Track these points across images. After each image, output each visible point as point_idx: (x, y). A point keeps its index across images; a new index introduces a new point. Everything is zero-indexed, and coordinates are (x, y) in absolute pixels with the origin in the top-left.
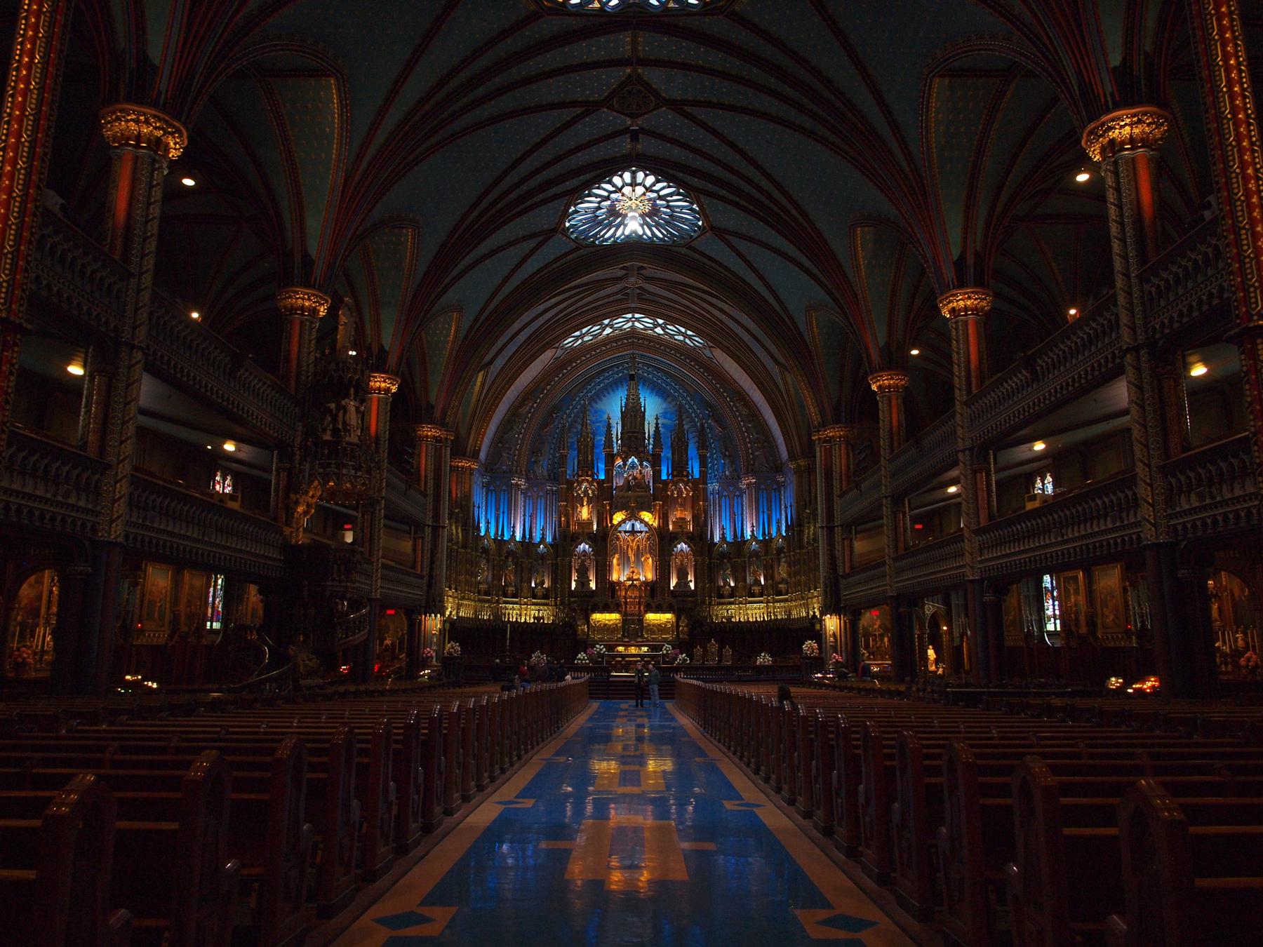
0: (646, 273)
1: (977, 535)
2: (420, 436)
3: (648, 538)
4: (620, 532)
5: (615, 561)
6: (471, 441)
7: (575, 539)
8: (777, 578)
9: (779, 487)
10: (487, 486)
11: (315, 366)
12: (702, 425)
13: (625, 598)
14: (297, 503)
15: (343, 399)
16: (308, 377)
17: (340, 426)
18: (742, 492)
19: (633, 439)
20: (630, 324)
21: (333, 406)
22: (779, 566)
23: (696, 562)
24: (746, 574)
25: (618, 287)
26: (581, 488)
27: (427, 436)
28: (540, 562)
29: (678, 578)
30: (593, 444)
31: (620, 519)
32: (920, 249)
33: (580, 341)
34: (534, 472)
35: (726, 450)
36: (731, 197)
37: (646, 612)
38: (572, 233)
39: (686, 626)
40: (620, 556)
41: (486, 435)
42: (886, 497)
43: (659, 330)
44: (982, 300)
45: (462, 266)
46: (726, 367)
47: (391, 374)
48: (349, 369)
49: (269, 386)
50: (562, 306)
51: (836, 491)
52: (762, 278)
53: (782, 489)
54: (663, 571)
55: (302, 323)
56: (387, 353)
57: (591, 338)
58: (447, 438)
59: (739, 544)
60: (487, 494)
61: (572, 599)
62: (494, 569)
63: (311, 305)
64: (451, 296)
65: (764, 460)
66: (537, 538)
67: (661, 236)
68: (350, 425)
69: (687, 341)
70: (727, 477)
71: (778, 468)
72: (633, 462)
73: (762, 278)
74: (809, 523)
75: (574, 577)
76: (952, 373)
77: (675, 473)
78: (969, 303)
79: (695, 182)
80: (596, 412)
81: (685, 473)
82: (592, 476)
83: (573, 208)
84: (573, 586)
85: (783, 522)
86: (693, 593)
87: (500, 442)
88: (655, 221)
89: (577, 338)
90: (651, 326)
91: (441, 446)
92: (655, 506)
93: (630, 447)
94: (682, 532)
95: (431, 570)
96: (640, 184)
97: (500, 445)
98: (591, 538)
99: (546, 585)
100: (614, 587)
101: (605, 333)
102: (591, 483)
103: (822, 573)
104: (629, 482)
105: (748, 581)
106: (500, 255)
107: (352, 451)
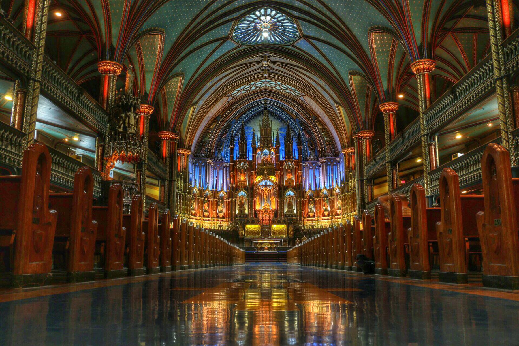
0: (272, 59)
1: (430, 175)
2: (163, 137)
3: (274, 189)
4: (260, 186)
5: (257, 200)
6: (187, 141)
7: (237, 189)
8: (336, 207)
9: (338, 163)
10: (195, 164)
11: (115, 97)
12: (299, 134)
13: (262, 217)
14: (107, 161)
15: (128, 112)
16: (112, 103)
17: (127, 125)
18: (319, 166)
20: (264, 85)
21: (123, 115)
22: (337, 200)
23: (297, 200)
24: (321, 205)
25: (258, 66)
26: (240, 165)
27: (166, 137)
28: (221, 200)
29: (288, 208)
30: (247, 143)
31: (259, 179)
32: (402, 42)
33: (240, 93)
35: (311, 146)
36: (312, 20)
37: (273, 224)
38: (236, 39)
39: (293, 231)
40: (260, 197)
41: (195, 139)
42: (388, 163)
43: (278, 88)
44: (431, 65)
45: (183, 54)
46: (311, 105)
47: (150, 105)
48: (131, 98)
49: (94, 106)
50: (231, 75)
51: (365, 162)
52: (328, 60)
54: (281, 204)
55: (109, 77)
56: (148, 95)
57: (245, 91)
58: (176, 138)
59: (317, 192)
62: (199, 203)
63: (113, 69)
64: (179, 69)
66: (219, 188)
67: (278, 40)
68: (131, 125)
69: (292, 92)
70: (312, 159)
71: (337, 154)
72: (266, 152)
73: (328, 60)
74: (351, 179)
75: (238, 207)
76: (418, 100)
77: (287, 157)
78: (425, 66)
79: (295, 13)
80: (248, 128)
81: (291, 157)
82: (246, 158)
83: (236, 27)
84: (237, 212)
85: (339, 180)
86: (296, 216)
87: (201, 142)
88: (276, 33)
89: (238, 91)
91: (173, 142)
92: (276, 173)
93: (264, 145)
95: (169, 201)
96: (269, 15)
98: (246, 189)
100: (257, 213)
101: (252, 89)
102: (245, 163)
103: (357, 203)
104: (264, 161)
105: (322, 209)
106: (202, 49)
107: (132, 137)
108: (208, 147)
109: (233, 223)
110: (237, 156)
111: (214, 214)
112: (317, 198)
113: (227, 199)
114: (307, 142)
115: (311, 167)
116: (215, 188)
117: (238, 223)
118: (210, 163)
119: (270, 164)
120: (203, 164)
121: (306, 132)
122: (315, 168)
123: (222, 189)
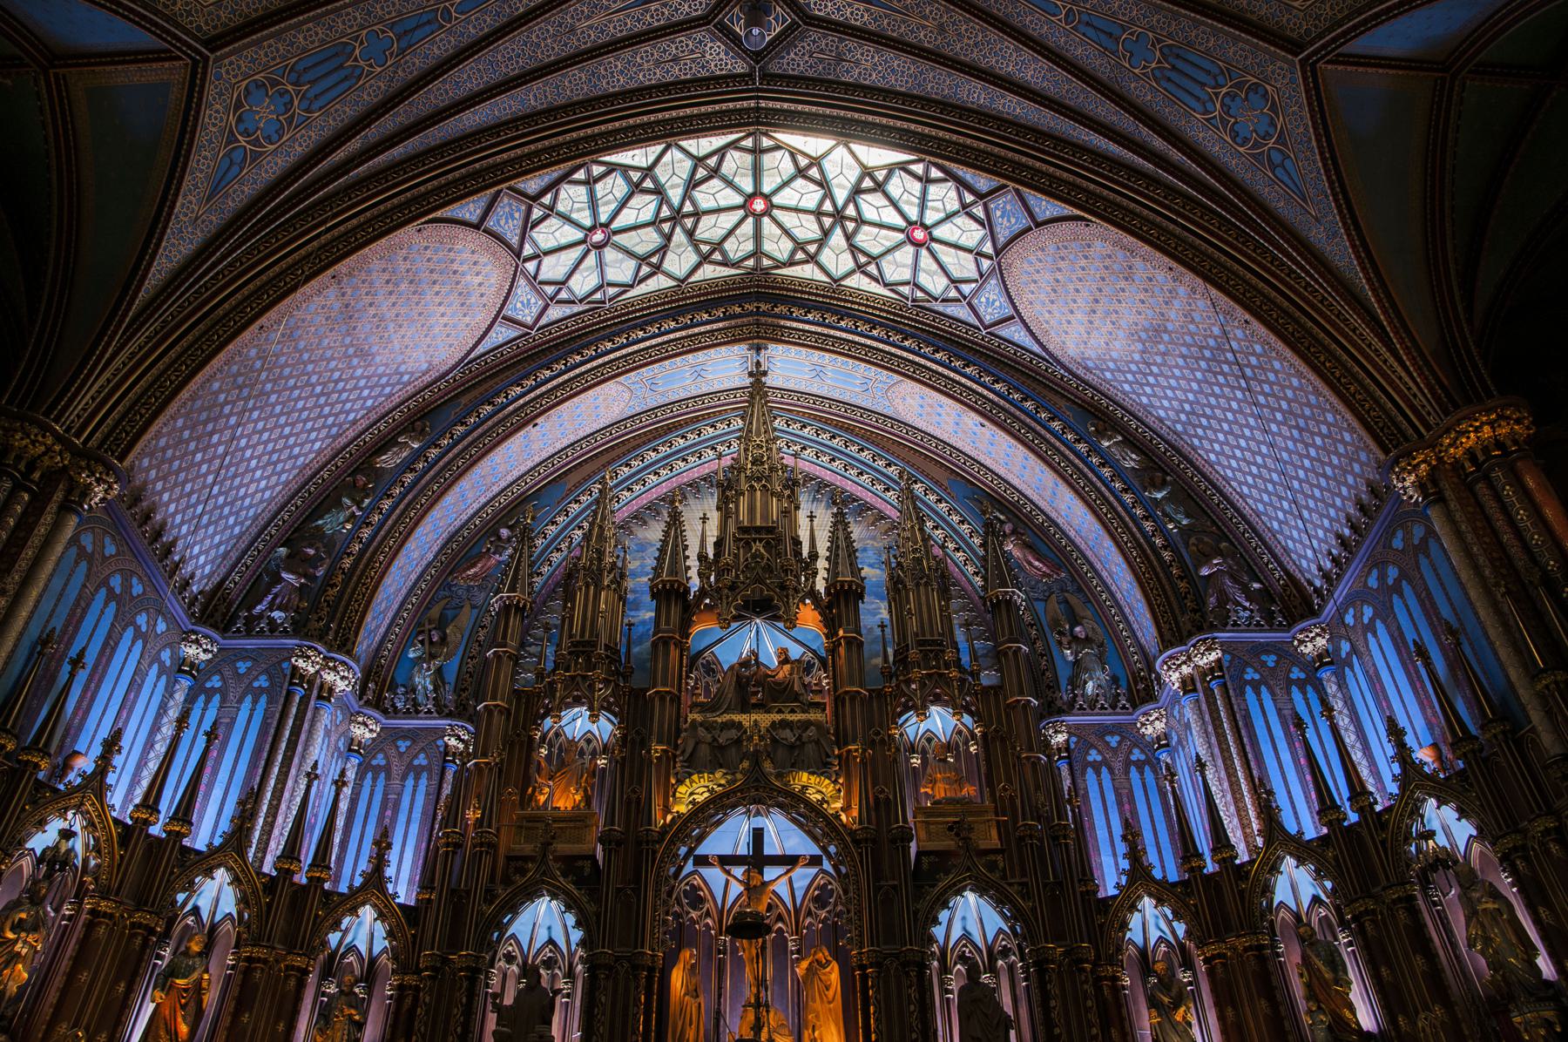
4: (703, 861)
5: (677, 978)
31: (700, 799)
35: (1075, 622)
43: (837, 259)
53: (1325, 675)
60: (190, 700)
70: (1092, 703)
90: (807, 229)
94: (966, 840)
97: (283, 551)
108: (330, 574)
114: (1039, 606)
115: (1094, 756)
116: (308, 853)
118: (326, 693)
119: (796, 700)
120: (263, 682)
121: (1027, 546)
122: (1128, 763)
123: (376, 880)
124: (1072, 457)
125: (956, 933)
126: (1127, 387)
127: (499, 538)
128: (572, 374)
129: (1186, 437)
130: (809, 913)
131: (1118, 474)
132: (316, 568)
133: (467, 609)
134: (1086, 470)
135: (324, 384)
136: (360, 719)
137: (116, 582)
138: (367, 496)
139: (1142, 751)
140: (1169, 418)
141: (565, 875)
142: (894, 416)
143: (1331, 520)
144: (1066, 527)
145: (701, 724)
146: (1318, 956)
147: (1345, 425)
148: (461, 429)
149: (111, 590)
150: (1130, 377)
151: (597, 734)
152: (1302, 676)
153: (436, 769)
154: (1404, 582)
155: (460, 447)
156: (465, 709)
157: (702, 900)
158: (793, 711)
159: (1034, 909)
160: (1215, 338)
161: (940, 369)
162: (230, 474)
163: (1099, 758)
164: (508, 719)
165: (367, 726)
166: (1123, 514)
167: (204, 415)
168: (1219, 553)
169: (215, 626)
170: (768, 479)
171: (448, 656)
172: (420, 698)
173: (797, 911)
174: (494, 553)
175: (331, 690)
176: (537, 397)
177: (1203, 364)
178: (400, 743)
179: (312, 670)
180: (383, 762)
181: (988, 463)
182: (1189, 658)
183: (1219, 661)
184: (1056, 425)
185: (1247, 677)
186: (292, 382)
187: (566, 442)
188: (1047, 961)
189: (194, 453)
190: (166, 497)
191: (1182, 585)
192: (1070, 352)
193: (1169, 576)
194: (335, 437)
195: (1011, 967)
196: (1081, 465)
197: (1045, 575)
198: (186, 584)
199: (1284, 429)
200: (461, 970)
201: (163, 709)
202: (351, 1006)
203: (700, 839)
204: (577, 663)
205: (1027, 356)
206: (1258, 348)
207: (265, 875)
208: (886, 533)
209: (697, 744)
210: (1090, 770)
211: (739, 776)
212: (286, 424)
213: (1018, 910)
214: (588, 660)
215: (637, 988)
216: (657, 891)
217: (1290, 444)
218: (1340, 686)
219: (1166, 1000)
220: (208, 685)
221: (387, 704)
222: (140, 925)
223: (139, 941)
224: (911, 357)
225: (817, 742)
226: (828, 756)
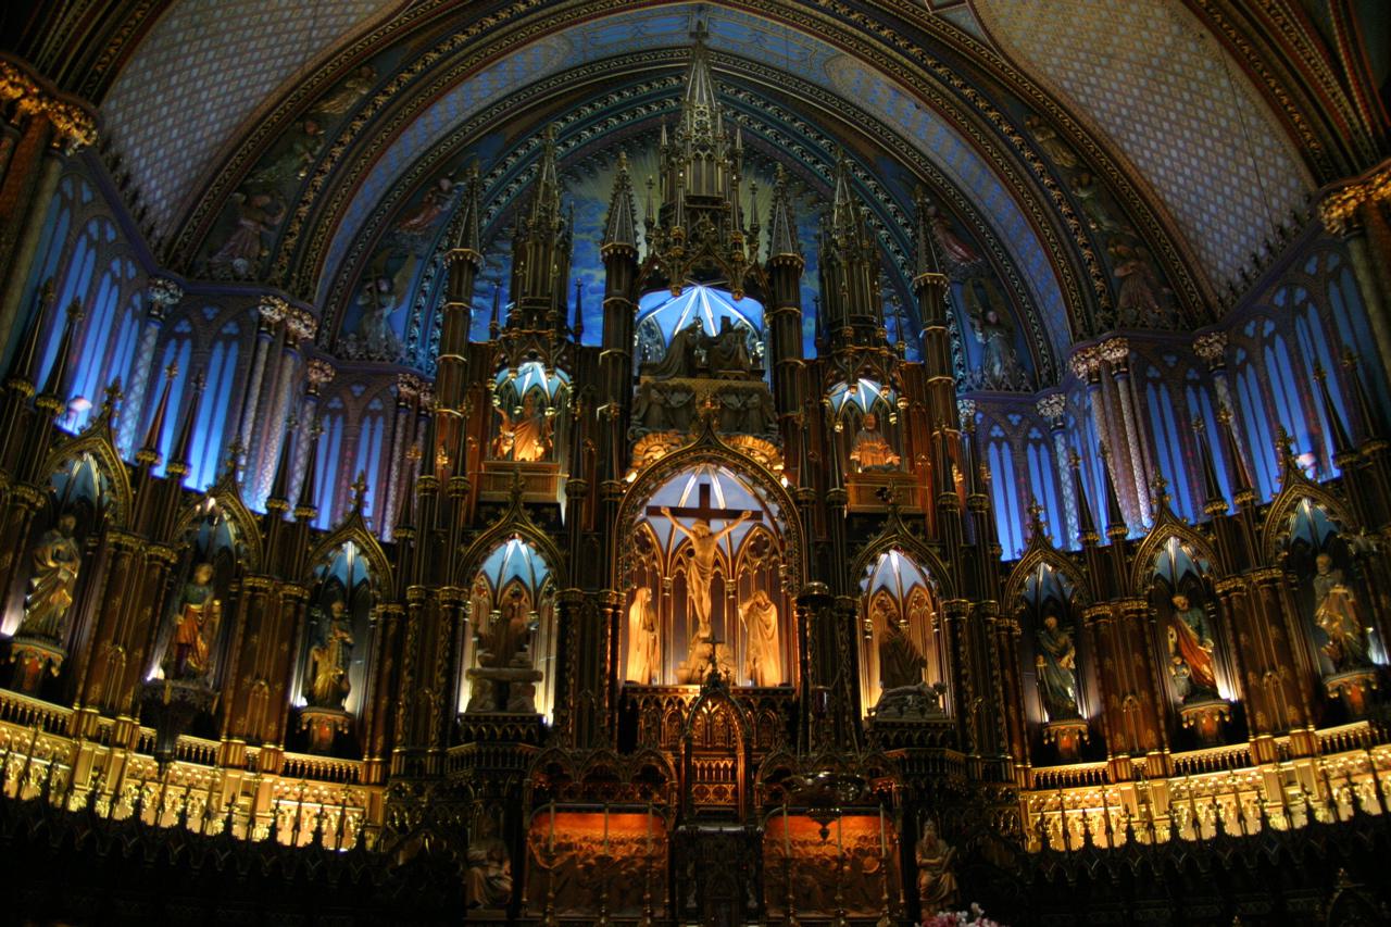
3: (758, 548)
4: (655, 511)
5: (636, 614)
19: (705, 218)
29: (888, 680)
34: (362, 337)
35: (987, 308)
60: (161, 344)
61: (453, 750)
65: (1152, 302)
77: (848, 330)
86: (956, 735)
87: (242, 189)
97: (240, 197)
99: (350, 704)
108: (287, 223)
109: (419, 791)
110: (494, 316)
111: (260, 714)
112: (1107, 600)
113: (388, 601)
115: (997, 432)
117: (463, 790)
120: (231, 328)
121: (950, 230)
122: (1026, 441)
123: (353, 523)
124: (1005, 149)
125: (876, 586)
126: (1066, 84)
127: (440, 189)
128: (517, 24)
129: (1117, 141)
130: (745, 560)
131: (1050, 169)
132: (274, 215)
133: (411, 257)
134: (1017, 163)
135: (275, 24)
136: (317, 364)
137: (93, 228)
138: (319, 143)
139: (1040, 431)
140: (1104, 120)
141: (535, 521)
142: (829, 88)
143: (1249, 238)
144: (987, 214)
145: (654, 387)
146: (1188, 621)
147: (1280, 151)
148: (406, 76)
149: (90, 238)
150: (1071, 74)
151: (546, 387)
152: (1197, 377)
153: (391, 414)
154: (1310, 305)
155: (407, 95)
156: (414, 357)
157: (649, 545)
158: (737, 378)
159: (950, 570)
160: (1166, 48)
161: (884, 47)
162: (187, 117)
163: (1001, 434)
164: (465, 373)
165: (322, 370)
166: (1049, 209)
167: (163, 56)
168: (1138, 258)
169: (179, 271)
170: (714, 148)
171: (397, 305)
172: (371, 346)
173: (734, 559)
174: (437, 203)
175: (295, 339)
176: (483, 46)
177: (1149, 72)
178: (355, 388)
179: (277, 318)
180: (340, 406)
181: (918, 144)
182: (1098, 353)
183: (1126, 358)
184: (992, 115)
185: (1150, 375)
186: (245, 21)
187: (504, 92)
188: (960, 614)
189: (155, 95)
190: (131, 140)
191: (1098, 284)
192: (1015, 43)
193: (1086, 273)
194: (287, 78)
195: (924, 616)
196: (1013, 158)
197: (963, 259)
198: (152, 229)
199: (1219, 147)
200: (444, 602)
201: (137, 354)
202: (342, 630)
203: (652, 493)
204: (531, 322)
205: (971, 42)
206: (1208, 64)
207: (259, 514)
208: (812, 205)
209: (649, 405)
210: (992, 445)
211: (691, 436)
212: (239, 66)
213: (936, 568)
214: (541, 318)
215: (605, 622)
216: (619, 538)
217: (1221, 160)
218: (1229, 390)
219: (1053, 649)
220: (178, 329)
221: (340, 350)
222: (157, 558)
223: (157, 572)
224: (855, 31)
225: (761, 410)
226: (770, 422)
